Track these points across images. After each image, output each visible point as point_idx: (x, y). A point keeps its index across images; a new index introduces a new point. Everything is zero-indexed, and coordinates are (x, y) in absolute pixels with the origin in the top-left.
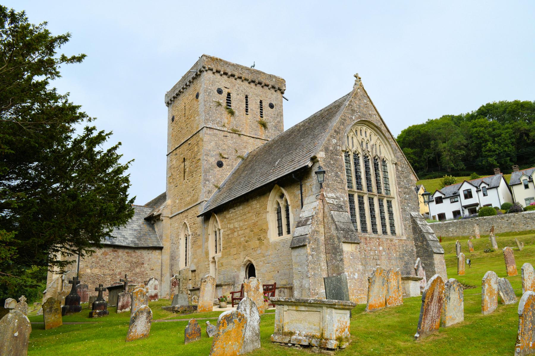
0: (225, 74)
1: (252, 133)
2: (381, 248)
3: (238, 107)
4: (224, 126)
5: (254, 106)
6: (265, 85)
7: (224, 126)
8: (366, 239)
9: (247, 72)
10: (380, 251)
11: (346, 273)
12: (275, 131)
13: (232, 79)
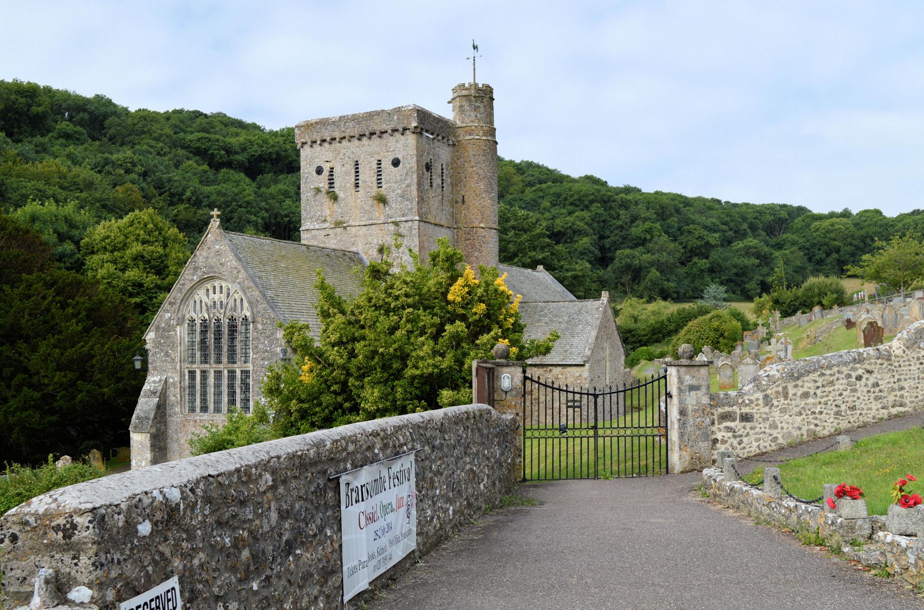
0: (324, 141)
1: (365, 218)
4: (325, 220)
5: (368, 176)
6: (382, 133)
7: (325, 220)
8: (196, 421)
9: (351, 124)
12: (401, 202)
13: (336, 145)
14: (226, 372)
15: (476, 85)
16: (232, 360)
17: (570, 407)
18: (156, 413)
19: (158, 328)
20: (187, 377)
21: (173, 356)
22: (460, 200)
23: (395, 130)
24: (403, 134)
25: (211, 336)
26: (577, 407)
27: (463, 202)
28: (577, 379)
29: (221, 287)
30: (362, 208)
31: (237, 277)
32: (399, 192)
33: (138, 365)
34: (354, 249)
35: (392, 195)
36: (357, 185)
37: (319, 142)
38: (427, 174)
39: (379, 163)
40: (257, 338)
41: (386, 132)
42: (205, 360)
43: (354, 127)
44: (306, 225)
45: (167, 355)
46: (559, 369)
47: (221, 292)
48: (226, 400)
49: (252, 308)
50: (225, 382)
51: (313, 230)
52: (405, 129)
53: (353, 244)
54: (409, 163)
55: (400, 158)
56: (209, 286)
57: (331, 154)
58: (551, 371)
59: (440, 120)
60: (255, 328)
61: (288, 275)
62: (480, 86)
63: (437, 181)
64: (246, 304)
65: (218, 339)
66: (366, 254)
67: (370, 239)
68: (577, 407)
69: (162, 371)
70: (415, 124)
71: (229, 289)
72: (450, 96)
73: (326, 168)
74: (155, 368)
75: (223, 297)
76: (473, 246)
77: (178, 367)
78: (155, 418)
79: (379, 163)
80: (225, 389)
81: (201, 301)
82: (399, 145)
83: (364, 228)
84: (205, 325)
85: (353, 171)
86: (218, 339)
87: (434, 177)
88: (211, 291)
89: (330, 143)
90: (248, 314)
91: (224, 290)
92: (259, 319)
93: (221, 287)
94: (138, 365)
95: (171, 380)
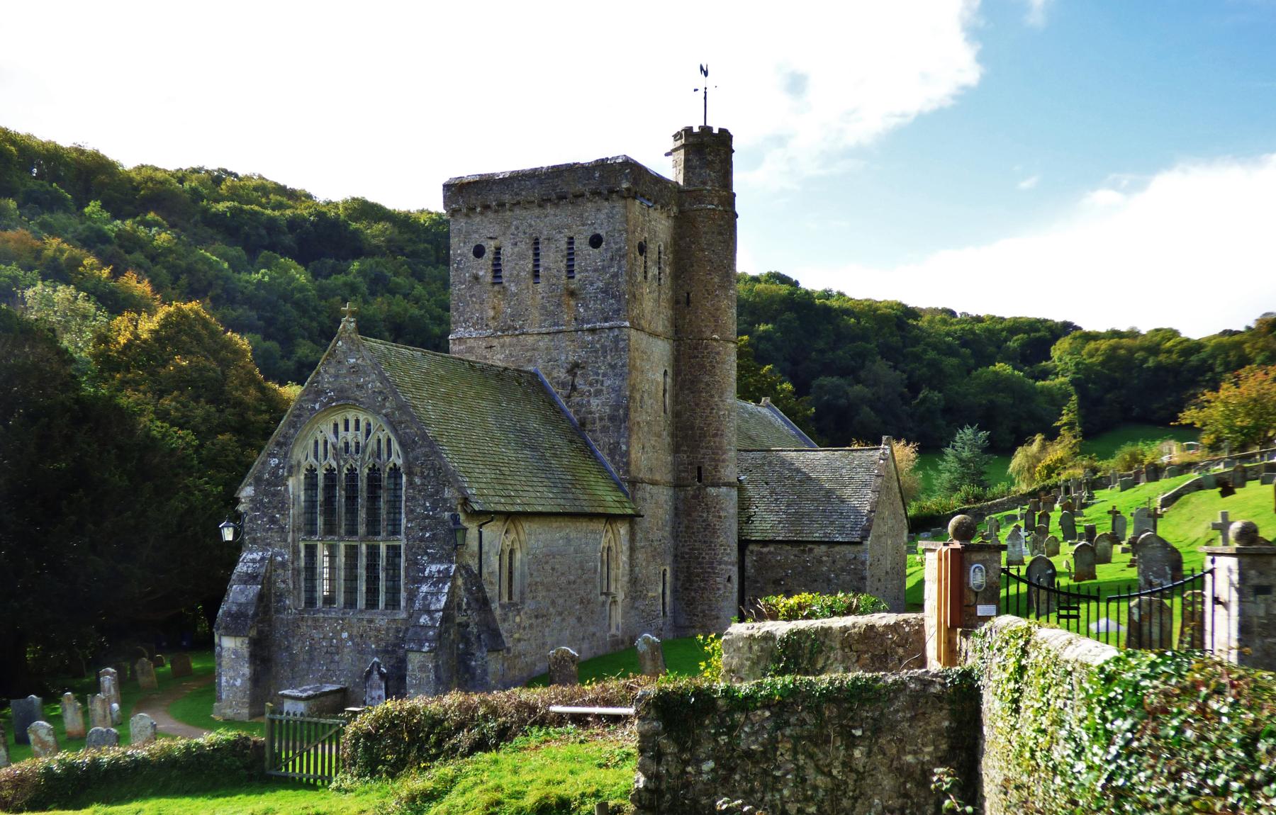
2: (345, 635)
3: (515, 273)
5: (552, 259)
6: (576, 196)
10: (342, 640)
11: (224, 679)
12: (603, 301)
14: (364, 547)
15: (710, 129)
16: (373, 529)
17: (1063, 617)
18: (257, 607)
19: (258, 481)
20: (302, 555)
21: (282, 522)
22: (683, 300)
23: (595, 193)
24: (607, 199)
25: (340, 494)
26: (1073, 617)
27: (688, 302)
28: (849, 562)
29: (357, 422)
30: (544, 307)
31: (383, 406)
32: (601, 285)
33: (228, 535)
34: (531, 368)
35: (590, 289)
36: (536, 275)
37: (478, 210)
38: (641, 259)
39: (571, 241)
40: (414, 498)
41: (582, 195)
42: (330, 529)
43: (533, 187)
44: (458, 332)
45: (273, 520)
46: (824, 548)
47: (357, 428)
48: (364, 589)
49: (406, 453)
50: (362, 562)
51: (467, 339)
52: (611, 191)
53: (530, 361)
54: (616, 243)
55: (602, 233)
56: (339, 419)
57: (497, 227)
58: (811, 550)
59: (659, 180)
60: (411, 483)
61: (450, 403)
62: (716, 131)
63: (653, 271)
64: (395, 446)
65: (352, 498)
66: (549, 375)
67: (554, 354)
68: (1073, 617)
69: (265, 545)
70: (625, 185)
71: (369, 425)
72: (671, 144)
73: (490, 246)
74: (254, 541)
75: (361, 438)
76: (702, 366)
77: (290, 540)
78: (256, 614)
79: (571, 241)
80: (362, 572)
81: (326, 442)
82: (602, 216)
83: (547, 338)
84: (331, 475)
85: (531, 252)
86: (352, 498)
87: (649, 264)
88: (341, 428)
89: (496, 211)
90: (400, 462)
91: (363, 425)
92: (418, 470)
93: (357, 422)
94: (228, 535)
95: (279, 559)
